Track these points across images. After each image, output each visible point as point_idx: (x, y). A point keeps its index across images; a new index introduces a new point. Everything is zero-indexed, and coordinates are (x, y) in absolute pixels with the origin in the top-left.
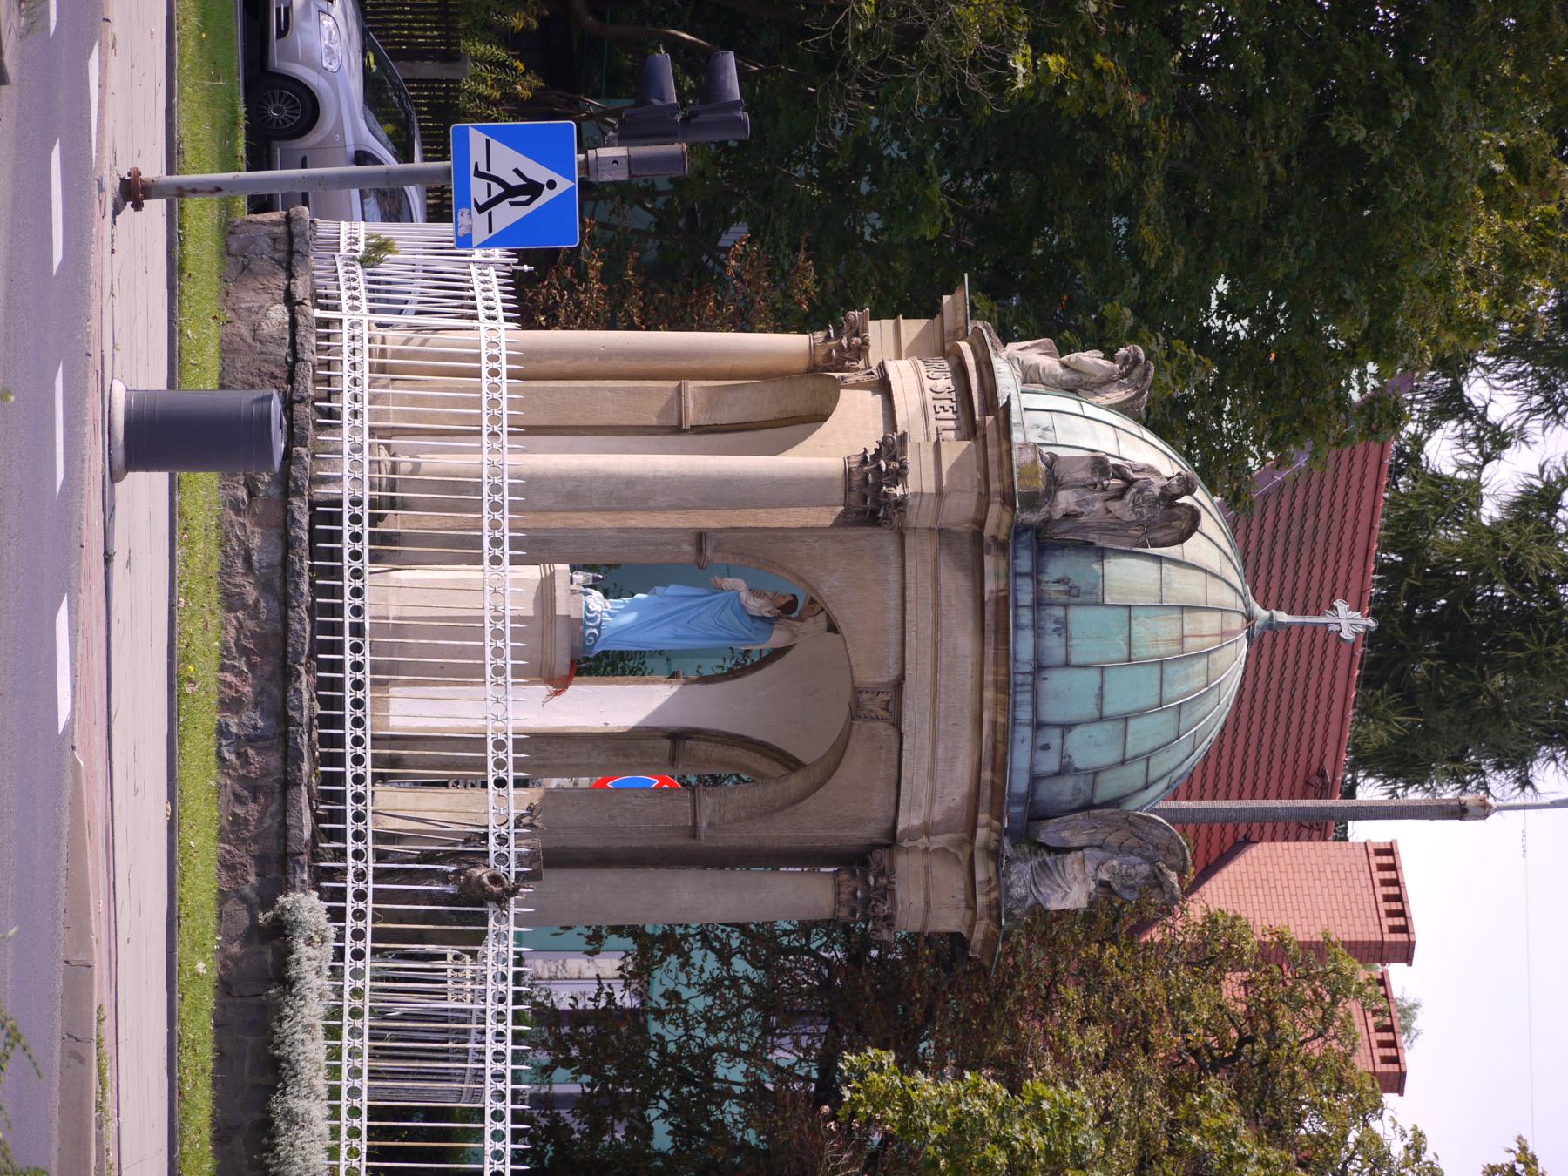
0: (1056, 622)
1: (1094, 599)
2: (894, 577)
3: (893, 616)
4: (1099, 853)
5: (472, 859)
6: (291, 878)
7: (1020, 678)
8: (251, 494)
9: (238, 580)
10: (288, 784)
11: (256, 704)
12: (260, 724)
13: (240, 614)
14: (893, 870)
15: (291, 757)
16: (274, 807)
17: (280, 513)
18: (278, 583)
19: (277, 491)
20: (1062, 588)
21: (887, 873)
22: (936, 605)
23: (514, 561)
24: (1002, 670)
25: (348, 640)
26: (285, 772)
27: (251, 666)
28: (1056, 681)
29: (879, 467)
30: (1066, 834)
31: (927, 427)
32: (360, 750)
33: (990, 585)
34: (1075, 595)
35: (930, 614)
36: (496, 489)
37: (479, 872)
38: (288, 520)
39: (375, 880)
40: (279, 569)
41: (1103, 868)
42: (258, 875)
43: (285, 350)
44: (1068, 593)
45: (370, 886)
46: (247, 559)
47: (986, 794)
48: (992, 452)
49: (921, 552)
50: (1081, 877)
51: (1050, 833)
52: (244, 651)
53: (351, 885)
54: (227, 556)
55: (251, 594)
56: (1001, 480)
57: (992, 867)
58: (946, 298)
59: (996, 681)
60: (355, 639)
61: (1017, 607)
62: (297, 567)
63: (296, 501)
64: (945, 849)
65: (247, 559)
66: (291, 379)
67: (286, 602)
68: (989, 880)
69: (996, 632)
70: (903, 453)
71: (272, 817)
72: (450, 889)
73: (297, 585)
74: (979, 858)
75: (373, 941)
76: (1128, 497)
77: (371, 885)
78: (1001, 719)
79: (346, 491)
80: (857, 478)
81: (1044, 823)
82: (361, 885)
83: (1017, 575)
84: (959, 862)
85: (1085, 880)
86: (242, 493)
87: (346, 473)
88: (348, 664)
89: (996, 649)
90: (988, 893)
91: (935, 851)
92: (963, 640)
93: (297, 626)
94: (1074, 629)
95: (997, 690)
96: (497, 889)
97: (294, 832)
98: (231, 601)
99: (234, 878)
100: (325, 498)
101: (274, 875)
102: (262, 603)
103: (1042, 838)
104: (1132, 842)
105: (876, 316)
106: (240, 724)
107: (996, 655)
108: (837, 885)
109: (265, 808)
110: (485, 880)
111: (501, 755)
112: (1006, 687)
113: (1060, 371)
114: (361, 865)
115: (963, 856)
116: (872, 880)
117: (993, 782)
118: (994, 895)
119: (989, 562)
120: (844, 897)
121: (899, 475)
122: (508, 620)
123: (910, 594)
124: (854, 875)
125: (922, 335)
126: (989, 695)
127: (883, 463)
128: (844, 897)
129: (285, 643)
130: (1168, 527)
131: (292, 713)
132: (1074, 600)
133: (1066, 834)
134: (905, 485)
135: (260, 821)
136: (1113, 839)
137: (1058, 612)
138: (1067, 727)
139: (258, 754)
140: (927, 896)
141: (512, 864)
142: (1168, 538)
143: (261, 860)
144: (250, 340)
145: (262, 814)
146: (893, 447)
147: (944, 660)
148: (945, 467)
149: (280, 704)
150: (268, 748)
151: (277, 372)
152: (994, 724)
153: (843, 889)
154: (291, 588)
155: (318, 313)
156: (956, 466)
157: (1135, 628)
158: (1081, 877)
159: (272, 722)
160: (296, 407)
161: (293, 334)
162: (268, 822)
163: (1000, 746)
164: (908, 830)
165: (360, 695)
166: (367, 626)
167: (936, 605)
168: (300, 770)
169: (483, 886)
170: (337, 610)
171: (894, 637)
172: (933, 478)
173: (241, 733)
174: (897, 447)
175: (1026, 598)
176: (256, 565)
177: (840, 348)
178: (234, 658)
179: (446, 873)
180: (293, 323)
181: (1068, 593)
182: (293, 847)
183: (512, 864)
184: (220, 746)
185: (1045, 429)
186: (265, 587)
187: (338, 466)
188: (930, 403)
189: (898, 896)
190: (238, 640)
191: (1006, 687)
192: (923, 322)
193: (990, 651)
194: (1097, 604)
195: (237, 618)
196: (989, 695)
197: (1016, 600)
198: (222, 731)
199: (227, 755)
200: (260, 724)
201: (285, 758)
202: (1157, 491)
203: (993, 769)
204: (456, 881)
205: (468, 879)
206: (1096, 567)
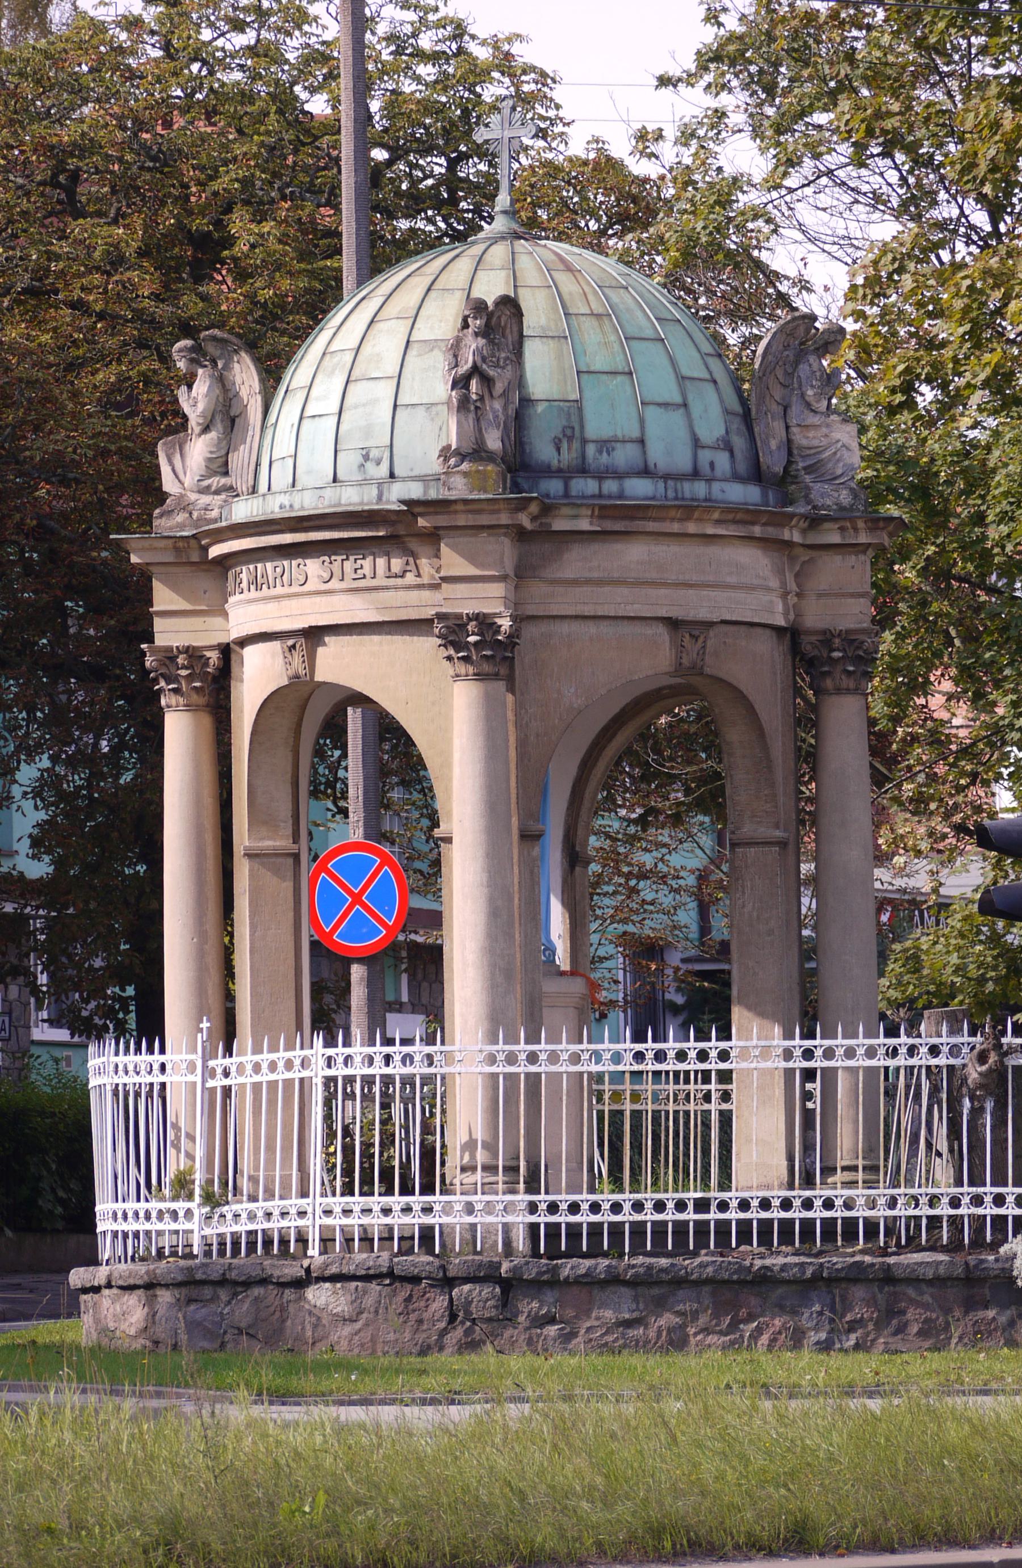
0: (600, 452)
1: (574, 411)
2: (565, 628)
3: (606, 629)
4: (795, 409)
5: (957, 1083)
6: (992, 1274)
7: (671, 494)
8: (552, 1320)
9: (652, 1334)
10: (888, 1278)
11: (794, 1312)
12: (817, 1308)
13: (691, 1331)
14: (824, 632)
15: (856, 1275)
16: (911, 1292)
17: (575, 1290)
18: (656, 1291)
19: (549, 1293)
20: (565, 445)
21: (827, 637)
22: (600, 582)
24: (672, 513)
25: (713, 1215)
26: (873, 1280)
27: (751, 1318)
28: (657, 454)
29: (476, 644)
30: (773, 444)
32: (606, 1206)
33: (584, 525)
34: (572, 431)
35: (607, 589)
36: (511, 1059)
37: (975, 1075)
38: (588, 1282)
39: (1005, 1184)
40: (640, 1290)
41: (815, 405)
42: (986, 1308)
43: (374, 1287)
44: (570, 439)
45: (989, 1190)
46: (628, 1324)
47: (771, 532)
48: (461, 520)
49: (543, 598)
50: (824, 430)
51: (774, 462)
52: (733, 1327)
53: (989, 1210)
54: (624, 1346)
55: (667, 1319)
56: (498, 511)
57: (827, 525)
58: (134, 559)
59: (681, 520)
60: (713, 1208)
61: (600, 496)
62: (641, 1270)
63: (565, 1272)
64: (797, 575)
65: (628, 1324)
66: (415, 1280)
67: (680, 1282)
68: (842, 529)
69: (633, 518)
70: (459, 616)
71: (922, 1294)
72: (989, 1105)
73: (662, 1270)
74: (814, 539)
75: (1006, 1185)
76: (491, 373)
77: (988, 1189)
78: (716, 515)
79: (521, 1219)
80: (486, 668)
81: (764, 467)
82: (988, 1199)
83: (566, 495)
84: (811, 560)
85: (828, 426)
86: (552, 1330)
87: (500, 1219)
88: (742, 1215)
89: (650, 519)
90: (856, 529)
91: (799, 586)
92: (634, 554)
93: (710, 1270)
94: (606, 433)
95: (688, 518)
96: (993, 1058)
97: (942, 1270)
98: (677, 1341)
99: (990, 1333)
100: (528, 1242)
101: (987, 1291)
102: (681, 1307)
103: (779, 469)
104: (780, 373)
105: (150, 639)
106: (817, 1329)
107: (655, 519)
108: (839, 691)
109: (912, 1301)
110: (984, 1068)
111: (861, 1051)
112: (689, 509)
113: (213, 435)
114: (966, 1200)
115: (805, 556)
116: (836, 654)
117: (764, 524)
118: (861, 524)
119: (559, 524)
120: (852, 685)
121: (485, 623)
123: (588, 610)
124: (828, 673)
125: (174, 587)
126: (692, 528)
127: (472, 639)
128: (852, 685)
129: (724, 1282)
130: (504, 329)
131: (809, 1273)
132: (577, 433)
133: (773, 444)
134: (499, 615)
135: (926, 1307)
136: (778, 393)
137: (591, 450)
138: (697, 444)
139: (851, 1309)
140: (852, 595)
141: (960, 1040)
142: (515, 329)
143: (970, 1305)
144: (358, 1325)
145: (918, 1304)
146: (451, 631)
147: (653, 575)
149: (794, 1287)
150: (844, 1299)
151: (404, 1294)
152: (719, 522)
153: (844, 685)
154: (664, 1277)
155: (313, 1251)
156: (473, 560)
157: (597, 367)
158: (824, 430)
159: (814, 1295)
160: (451, 1274)
161: (354, 1278)
162: (927, 1298)
163: (740, 516)
164: (786, 613)
165: (564, 1206)
166: (699, 1195)
167: (600, 582)
168: (873, 1265)
169: (990, 1071)
170: (680, 1227)
171: (626, 628)
172: (487, 585)
173: (827, 1327)
174: (450, 623)
175: (590, 486)
176: (635, 1315)
177: (190, 678)
178: (742, 1337)
179: (972, 1110)
180: (334, 1279)
181: (570, 439)
182: (959, 1271)
183: (960, 1040)
184: (841, 1350)
185: (366, 457)
186: (660, 1305)
187: (489, 1229)
188: (347, 584)
189: (852, 626)
190: (722, 1333)
191: (689, 509)
192: (156, 584)
193: (652, 526)
194: (580, 409)
195: (695, 1334)
196: (692, 528)
197: (593, 496)
198: (825, 1347)
199: (852, 1342)
200: (817, 1308)
201: (855, 1281)
202: (481, 341)
203: (753, 523)
204: (982, 1099)
205: (980, 1086)
206: (540, 408)
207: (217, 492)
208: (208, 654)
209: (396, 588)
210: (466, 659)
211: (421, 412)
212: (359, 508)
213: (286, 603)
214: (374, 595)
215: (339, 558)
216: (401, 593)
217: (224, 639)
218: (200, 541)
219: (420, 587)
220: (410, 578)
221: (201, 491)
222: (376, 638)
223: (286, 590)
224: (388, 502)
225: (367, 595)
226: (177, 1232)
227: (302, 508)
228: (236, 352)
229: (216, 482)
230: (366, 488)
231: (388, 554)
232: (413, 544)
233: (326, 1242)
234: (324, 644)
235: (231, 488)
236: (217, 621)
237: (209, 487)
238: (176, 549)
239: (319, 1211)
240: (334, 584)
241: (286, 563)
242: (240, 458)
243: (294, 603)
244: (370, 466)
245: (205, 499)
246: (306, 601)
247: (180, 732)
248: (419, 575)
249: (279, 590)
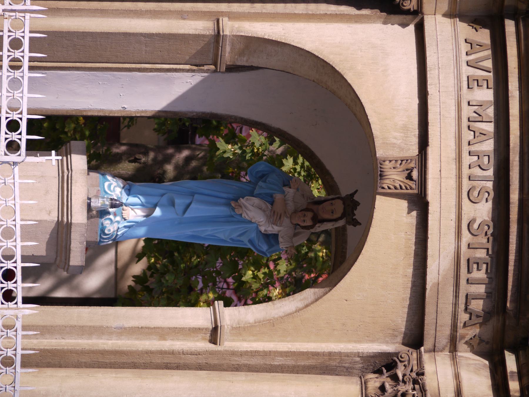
209: (456, 305)
213: (453, 166)
215: (489, 246)
216: (450, 308)
217: (427, 7)
219: (454, 327)
220: (464, 317)
223: (466, 171)
231: (489, 294)
232: (494, 322)
234: (410, 211)
236: (445, 7)
241: (490, 173)
243: (452, 183)
248: (465, 325)
249: (467, 160)
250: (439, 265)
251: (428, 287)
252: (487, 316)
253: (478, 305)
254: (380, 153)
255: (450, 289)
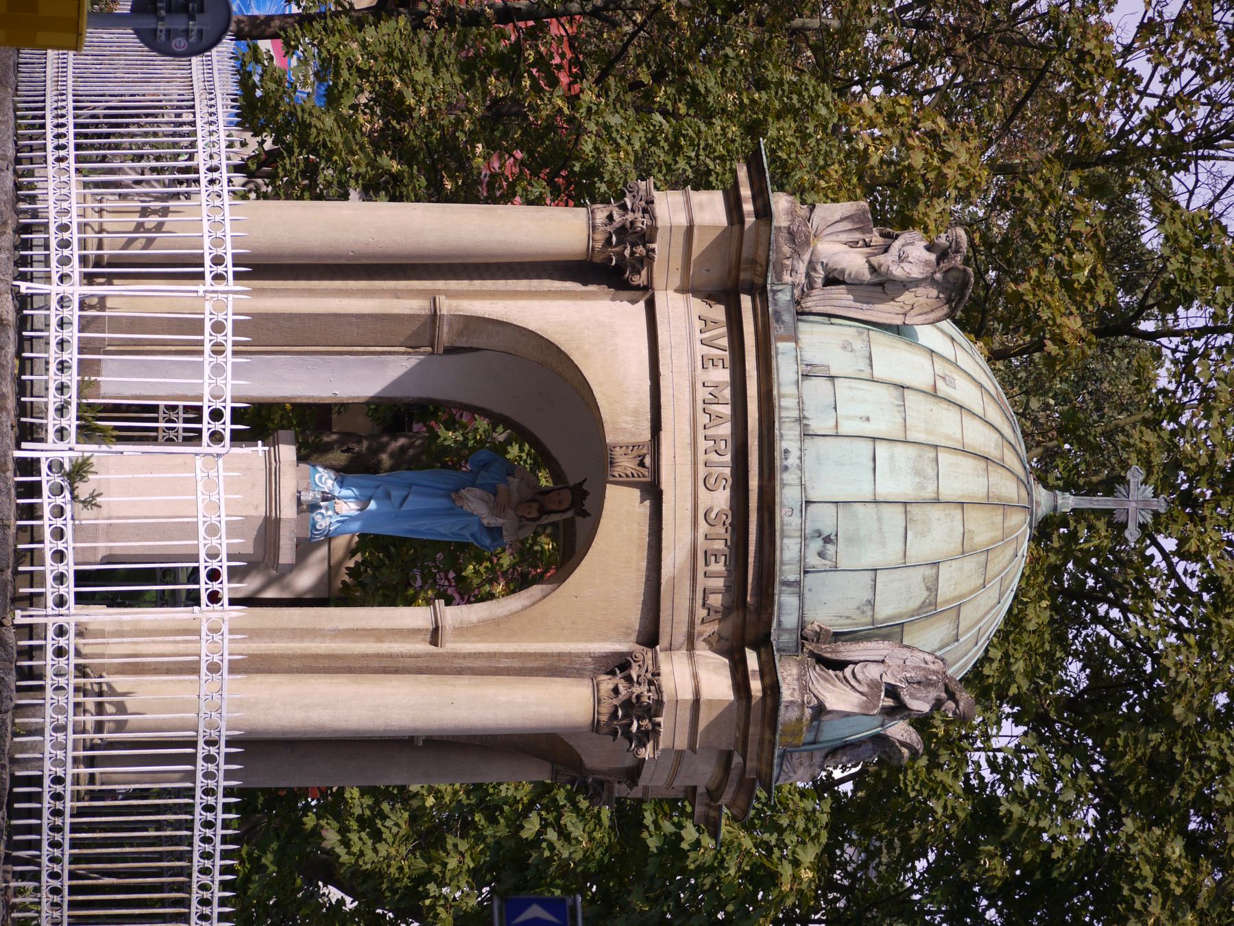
23: (237, 438)
31: (694, 591)
56: (759, 759)
122: (223, 743)
148: (702, 724)
155: (20, 618)
177: (621, 256)
185: (827, 540)
207: (808, 275)
208: (644, 272)
209: (693, 600)
210: (614, 715)
211: (868, 595)
212: (777, 499)
213: (689, 452)
214: (688, 575)
215: (728, 536)
216: (687, 604)
217: (658, 281)
218: (760, 292)
219: (692, 624)
220: (701, 613)
221: (810, 262)
222: (644, 564)
223: (701, 457)
224: (781, 592)
225: (688, 566)
226: (47, 247)
227: (783, 485)
228: (949, 301)
229: (819, 276)
230: (795, 568)
231: (728, 587)
232: (735, 618)
233: (30, 631)
234: (642, 500)
235: (811, 286)
236: (676, 281)
237: (815, 270)
238: (753, 262)
239: (60, 620)
240: (703, 527)
241: (728, 458)
242: (840, 298)
243: (687, 469)
244: (817, 545)
245: (802, 268)
246: (688, 490)
247: (563, 228)
248: (703, 622)
249: (703, 445)
250: (674, 558)
251: (663, 581)
252: (727, 611)
253: (716, 600)
254: (609, 439)
255: (687, 583)
